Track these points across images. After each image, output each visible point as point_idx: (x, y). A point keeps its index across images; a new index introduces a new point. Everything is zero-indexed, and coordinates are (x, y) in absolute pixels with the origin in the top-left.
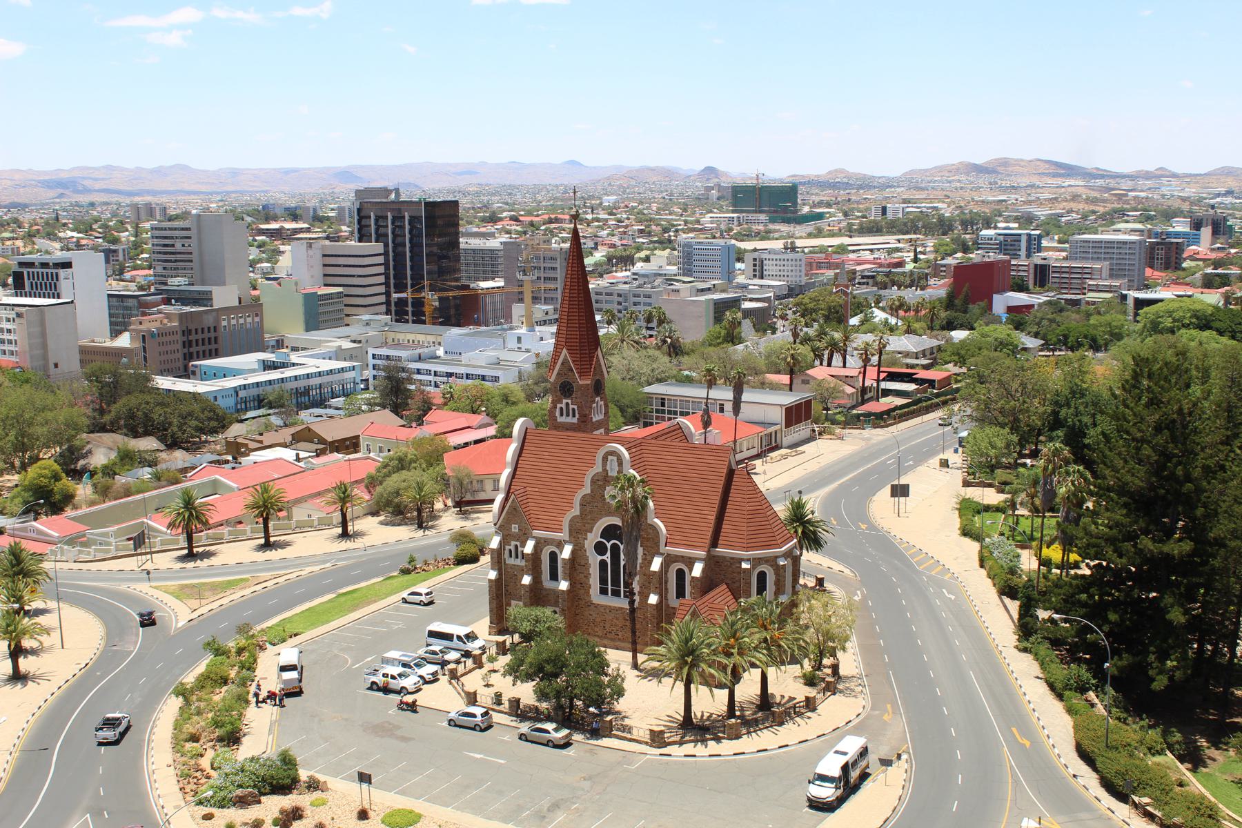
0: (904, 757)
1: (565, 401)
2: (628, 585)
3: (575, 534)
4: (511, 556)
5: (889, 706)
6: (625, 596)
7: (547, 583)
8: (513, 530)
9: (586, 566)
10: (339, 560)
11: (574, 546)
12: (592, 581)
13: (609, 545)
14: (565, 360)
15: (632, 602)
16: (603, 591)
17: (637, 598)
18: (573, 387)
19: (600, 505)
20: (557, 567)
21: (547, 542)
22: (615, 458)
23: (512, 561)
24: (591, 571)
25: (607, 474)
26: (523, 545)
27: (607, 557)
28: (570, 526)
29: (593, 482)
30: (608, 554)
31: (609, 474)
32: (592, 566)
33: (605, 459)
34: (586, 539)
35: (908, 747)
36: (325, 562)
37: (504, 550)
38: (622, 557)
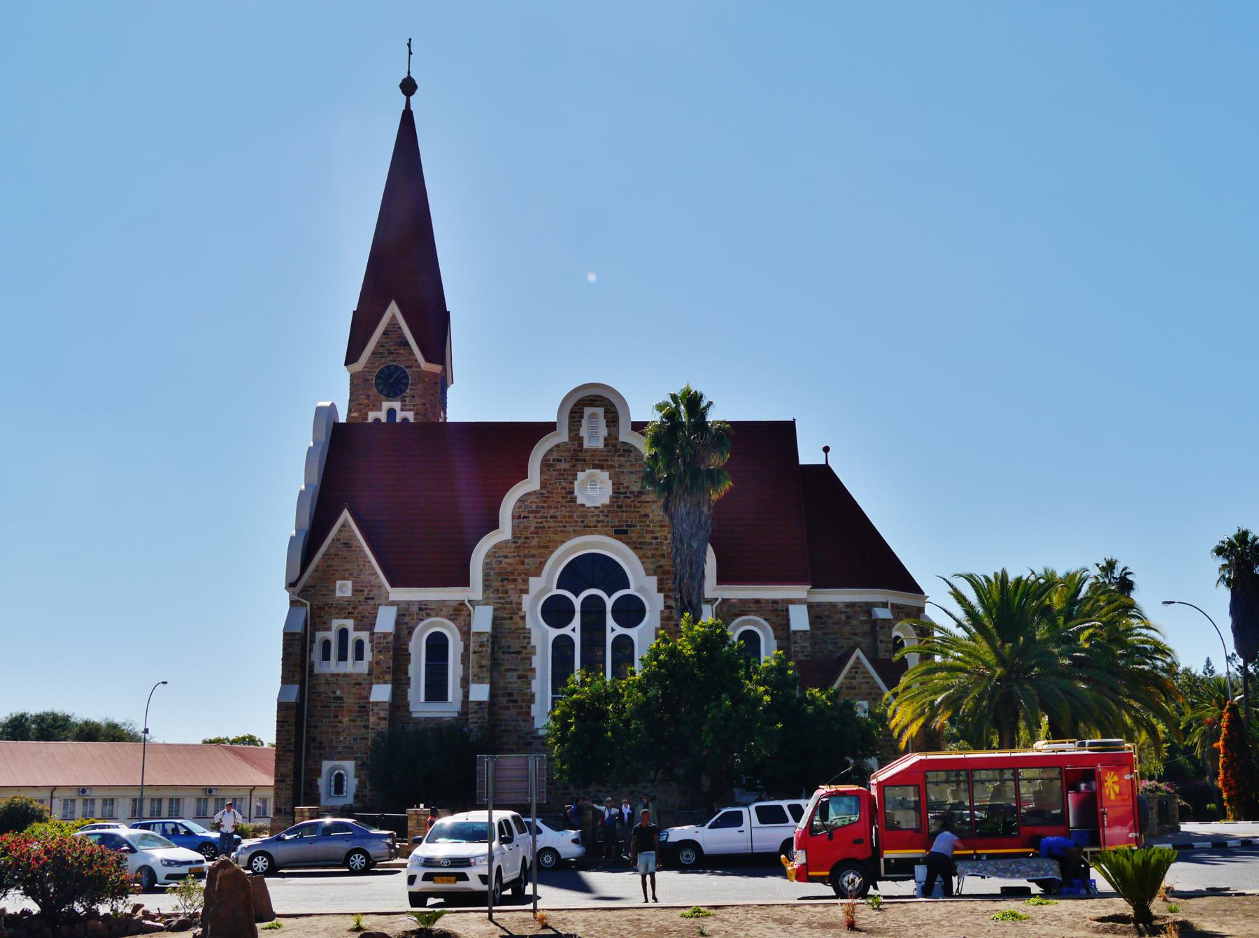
1: (386, 405)
3: (496, 584)
4: (326, 656)
7: (419, 705)
8: (338, 594)
9: (524, 652)
11: (495, 610)
12: (536, 686)
13: (577, 602)
14: (393, 325)
18: (406, 377)
19: (562, 512)
20: (446, 666)
21: (425, 610)
22: (600, 411)
23: (333, 666)
24: (536, 662)
25: (581, 444)
26: (366, 622)
27: (574, 630)
28: (487, 566)
29: (546, 465)
30: (576, 622)
31: (586, 445)
32: (538, 650)
34: (526, 591)
37: (313, 642)
38: (610, 622)
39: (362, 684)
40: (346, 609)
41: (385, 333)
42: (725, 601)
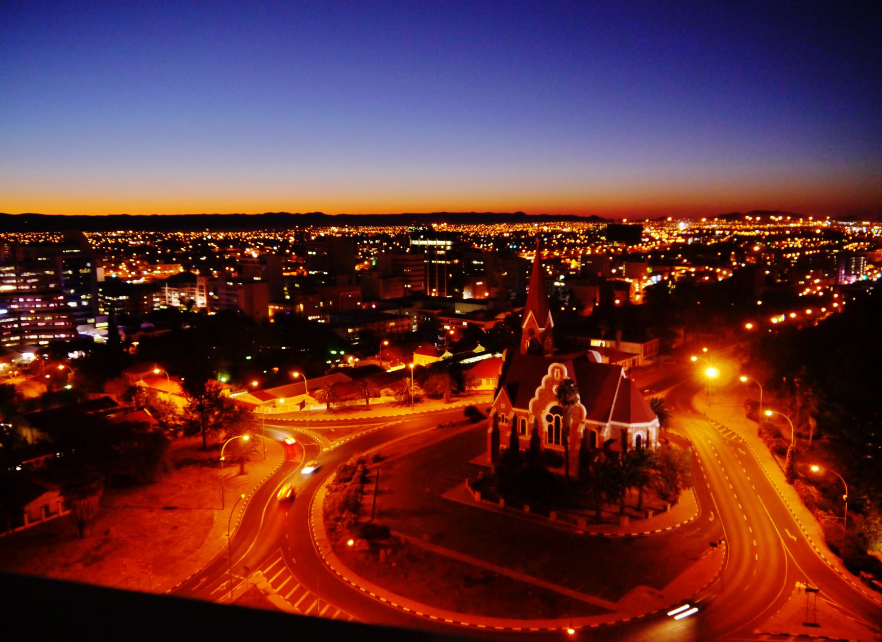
0: (723, 542)
2: (564, 439)
5: (712, 513)
6: (563, 444)
8: (502, 407)
9: (542, 427)
10: (406, 419)
13: (554, 417)
15: (566, 448)
16: (551, 441)
17: (569, 446)
21: (520, 414)
22: (559, 370)
26: (507, 414)
27: (553, 423)
29: (547, 382)
33: (553, 371)
35: (724, 537)
36: (398, 420)
38: (561, 423)
39: (506, 429)
40: (504, 411)
41: (530, 319)
42: (587, 423)
